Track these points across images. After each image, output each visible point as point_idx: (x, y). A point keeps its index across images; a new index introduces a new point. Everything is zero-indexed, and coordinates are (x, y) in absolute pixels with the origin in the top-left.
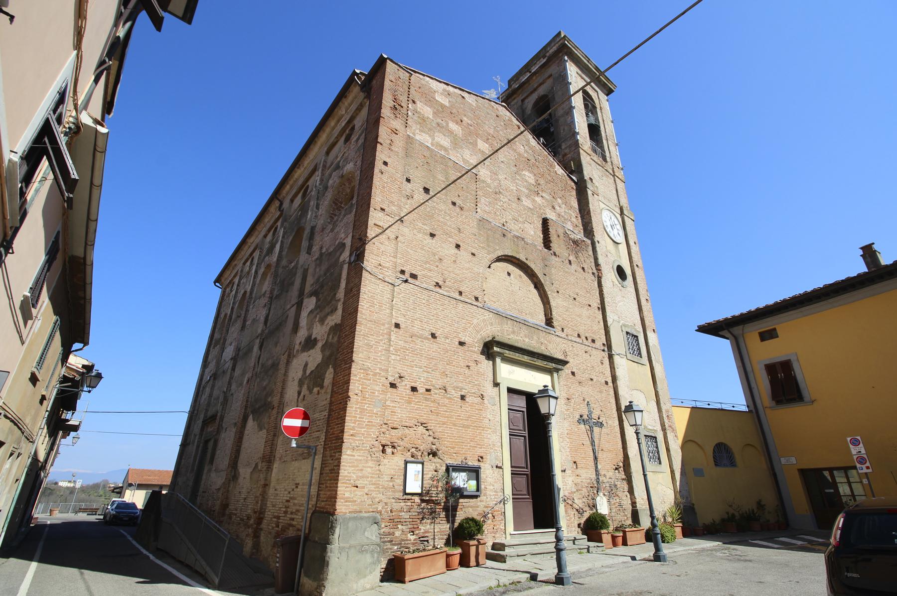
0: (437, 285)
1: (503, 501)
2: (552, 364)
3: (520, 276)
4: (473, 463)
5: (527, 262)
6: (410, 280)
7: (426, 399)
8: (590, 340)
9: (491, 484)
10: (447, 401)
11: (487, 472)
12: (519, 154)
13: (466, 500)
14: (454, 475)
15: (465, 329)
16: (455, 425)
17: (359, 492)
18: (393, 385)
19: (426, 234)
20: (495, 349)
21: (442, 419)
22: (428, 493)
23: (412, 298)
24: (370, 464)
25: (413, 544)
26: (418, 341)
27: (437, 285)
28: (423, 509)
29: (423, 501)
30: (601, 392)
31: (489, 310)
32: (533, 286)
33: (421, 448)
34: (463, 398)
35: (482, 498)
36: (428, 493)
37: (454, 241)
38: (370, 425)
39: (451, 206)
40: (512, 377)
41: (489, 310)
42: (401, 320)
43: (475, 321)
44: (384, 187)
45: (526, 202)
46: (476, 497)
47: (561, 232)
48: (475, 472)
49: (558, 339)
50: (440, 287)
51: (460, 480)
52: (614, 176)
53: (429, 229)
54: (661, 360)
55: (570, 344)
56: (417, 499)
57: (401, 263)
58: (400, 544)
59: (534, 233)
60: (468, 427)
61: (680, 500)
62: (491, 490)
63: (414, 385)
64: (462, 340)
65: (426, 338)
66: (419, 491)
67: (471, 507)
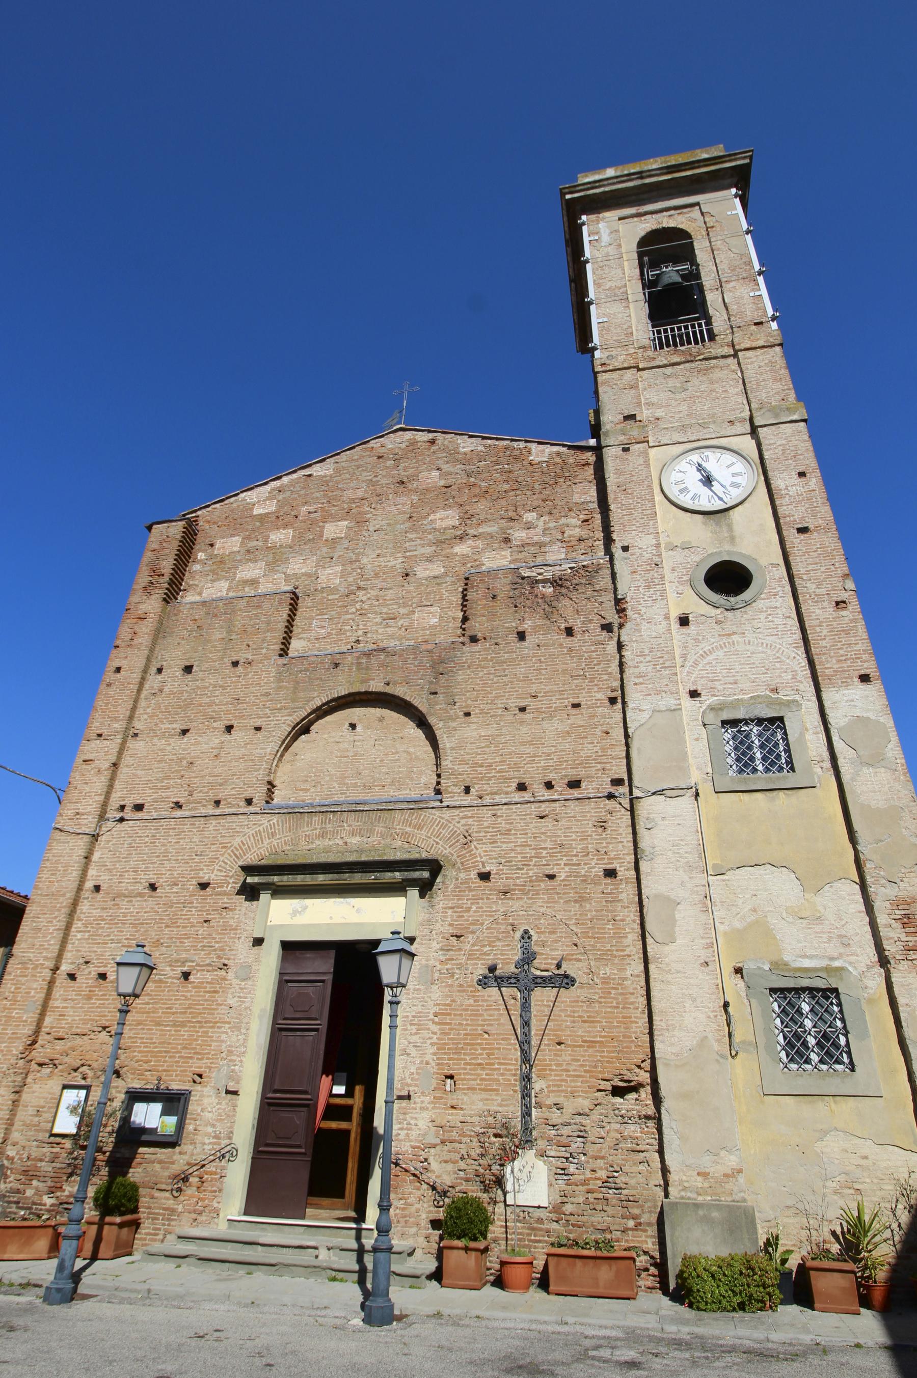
0: (178, 805)
1: (225, 1155)
2: (419, 875)
5: (388, 690)
8: (560, 785)
9: (208, 1124)
11: (206, 1101)
13: (152, 1150)
15: (213, 860)
16: (158, 1024)
23: (129, 840)
25: (49, 1211)
26: (123, 903)
27: (178, 805)
28: (75, 1159)
33: (95, 1065)
34: (186, 975)
35: (186, 1147)
37: (221, 725)
40: (300, 920)
43: (237, 841)
44: (107, 704)
45: (423, 571)
48: (175, 1102)
49: (447, 814)
50: (180, 807)
51: (148, 1115)
53: (179, 726)
55: (486, 813)
56: (68, 1144)
58: (30, 1208)
59: (436, 619)
60: (183, 1024)
62: (208, 1135)
64: (204, 881)
65: (140, 895)
67: (160, 1162)
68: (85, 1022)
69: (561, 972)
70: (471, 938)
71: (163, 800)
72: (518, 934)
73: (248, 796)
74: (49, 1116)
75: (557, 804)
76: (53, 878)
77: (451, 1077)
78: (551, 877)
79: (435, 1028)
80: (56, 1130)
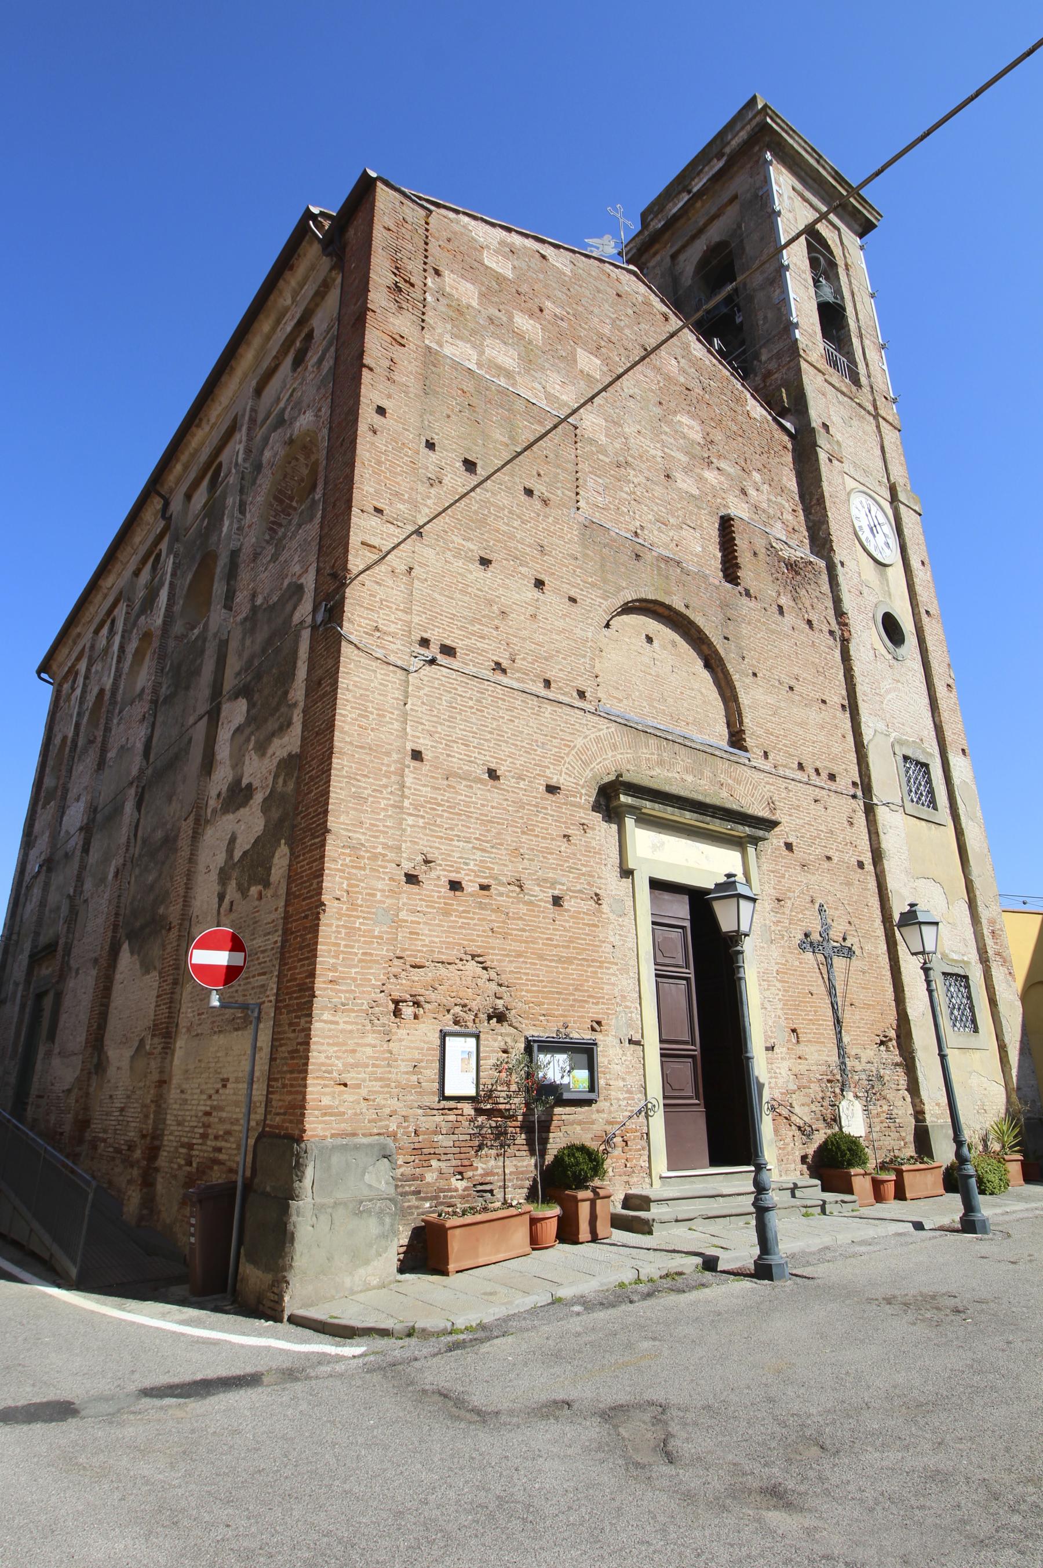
0: (498, 667)
1: (646, 1111)
2: (742, 828)
3: (674, 644)
4: (580, 1034)
6: (441, 659)
7: (482, 906)
8: (824, 775)
9: (618, 1077)
10: (523, 909)
11: (611, 1052)
12: (668, 378)
13: (568, 1110)
14: (543, 1058)
15: (558, 759)
16: (541, 957)
17: (349, 1096)
18: (412, 879)
19: (471, 560)
20: (623, 798)
21: (515, 946)
22: (489, 1095)
23: (446, 697)
24: (370, 1039)
25: (463, 1197)
26: (462, 786)
28: (481, 1127)
29: (479, 1112)
30: (849, 884)
31: (608, 717)
32: (700, 663)
33: (474, 1005)
34: (557, 901)
36: (489, 1095)
37: (530, 573)
38: (367, 960)
39: (523, 498)
40: (658, 856)
41: (608, 717)
42: (423, 744)
43: (579, 742)
45: (685, 483)
46: (589, 1102)
47: (760, 544)
48: (585, 1053)
49: (757, 775)
50: (504, 671)
51: (554, 1068)
52: (876, 416)
54: (979, 814)
55: (782, 783)
56: (468, 1109)
57: (421, 624)
58: (436, 1197)
59: (702, 549)
60: (569, 961)
61: (1018, 1105)
62: (620, 1089)
63: (454, 877)
64: (553, 782)
65: (480, 781)
66: (472, 1092)
67: (580, 1123)
68: (450, 946)
69: (848, 944)
70: (789, 903)
71: (481, 652)
72: (817, 906)
73: (582, 688)
74: (433, 1072)
75: (824, 792)
76: (363, 722)
77: (794, 1031)
78: (829, 858)
79: (779, 985)
80: (447, 1093)
